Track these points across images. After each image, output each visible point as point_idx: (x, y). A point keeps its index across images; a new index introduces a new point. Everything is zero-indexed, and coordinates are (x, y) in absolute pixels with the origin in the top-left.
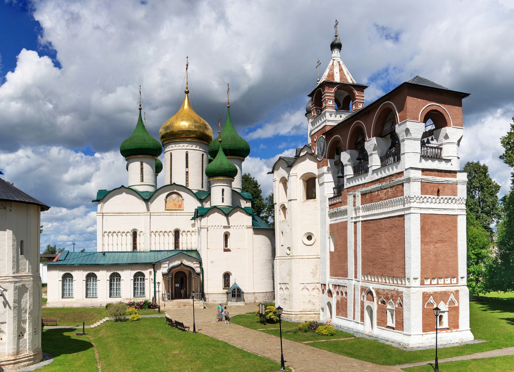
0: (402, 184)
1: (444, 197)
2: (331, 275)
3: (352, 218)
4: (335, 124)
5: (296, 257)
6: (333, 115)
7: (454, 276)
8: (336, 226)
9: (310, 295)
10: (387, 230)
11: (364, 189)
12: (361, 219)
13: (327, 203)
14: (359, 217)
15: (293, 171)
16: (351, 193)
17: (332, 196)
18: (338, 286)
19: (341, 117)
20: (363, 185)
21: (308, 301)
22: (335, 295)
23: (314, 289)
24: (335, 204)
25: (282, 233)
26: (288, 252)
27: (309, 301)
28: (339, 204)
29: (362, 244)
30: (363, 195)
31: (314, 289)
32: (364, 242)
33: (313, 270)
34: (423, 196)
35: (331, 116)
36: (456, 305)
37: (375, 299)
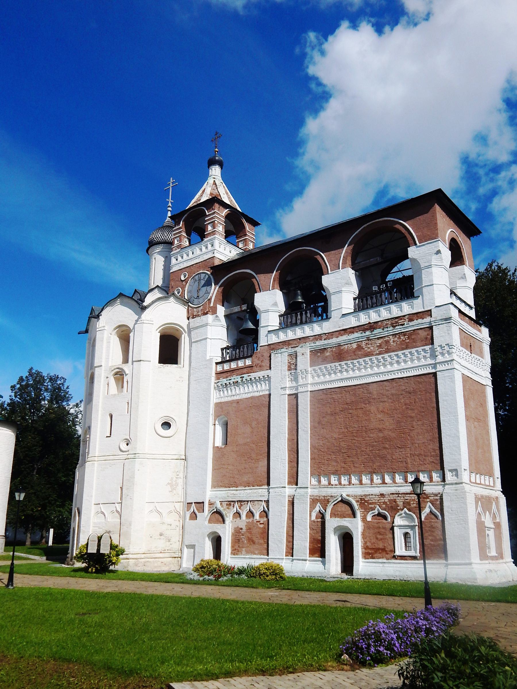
0: (431, 328)
1: (476, 356)
2: (213, 486)
3: (284, 388)
4: (225, 259)
5: (147, 456)
6: (222, 246)
7: (491, 474)
8: (235, 405)
9: (163, 523)
10: (386, 399)
11: (320, 343)
12: (310, 388)
13: (214, 369)
14: (306, 385)
15: (146, 315)
16: (283, 350)
17: (220, 360)
18: (241, 501)
19: (230, 252)
20: (319, 337)
21: (158, 533)
22: (229, 519)
23: (171, 512)
24: (232, 371)
25: (111, 417)
26: (124, 447)
27: (161, 535)
28: (245, 370)
29: (313, 428)
30: (314, 353)
31: (171, 512)
32: (318, 424)
33: (172, 478)
34: (461, 348)
35: (220, 247)
36: (498, 520)
37: (359, 514)
